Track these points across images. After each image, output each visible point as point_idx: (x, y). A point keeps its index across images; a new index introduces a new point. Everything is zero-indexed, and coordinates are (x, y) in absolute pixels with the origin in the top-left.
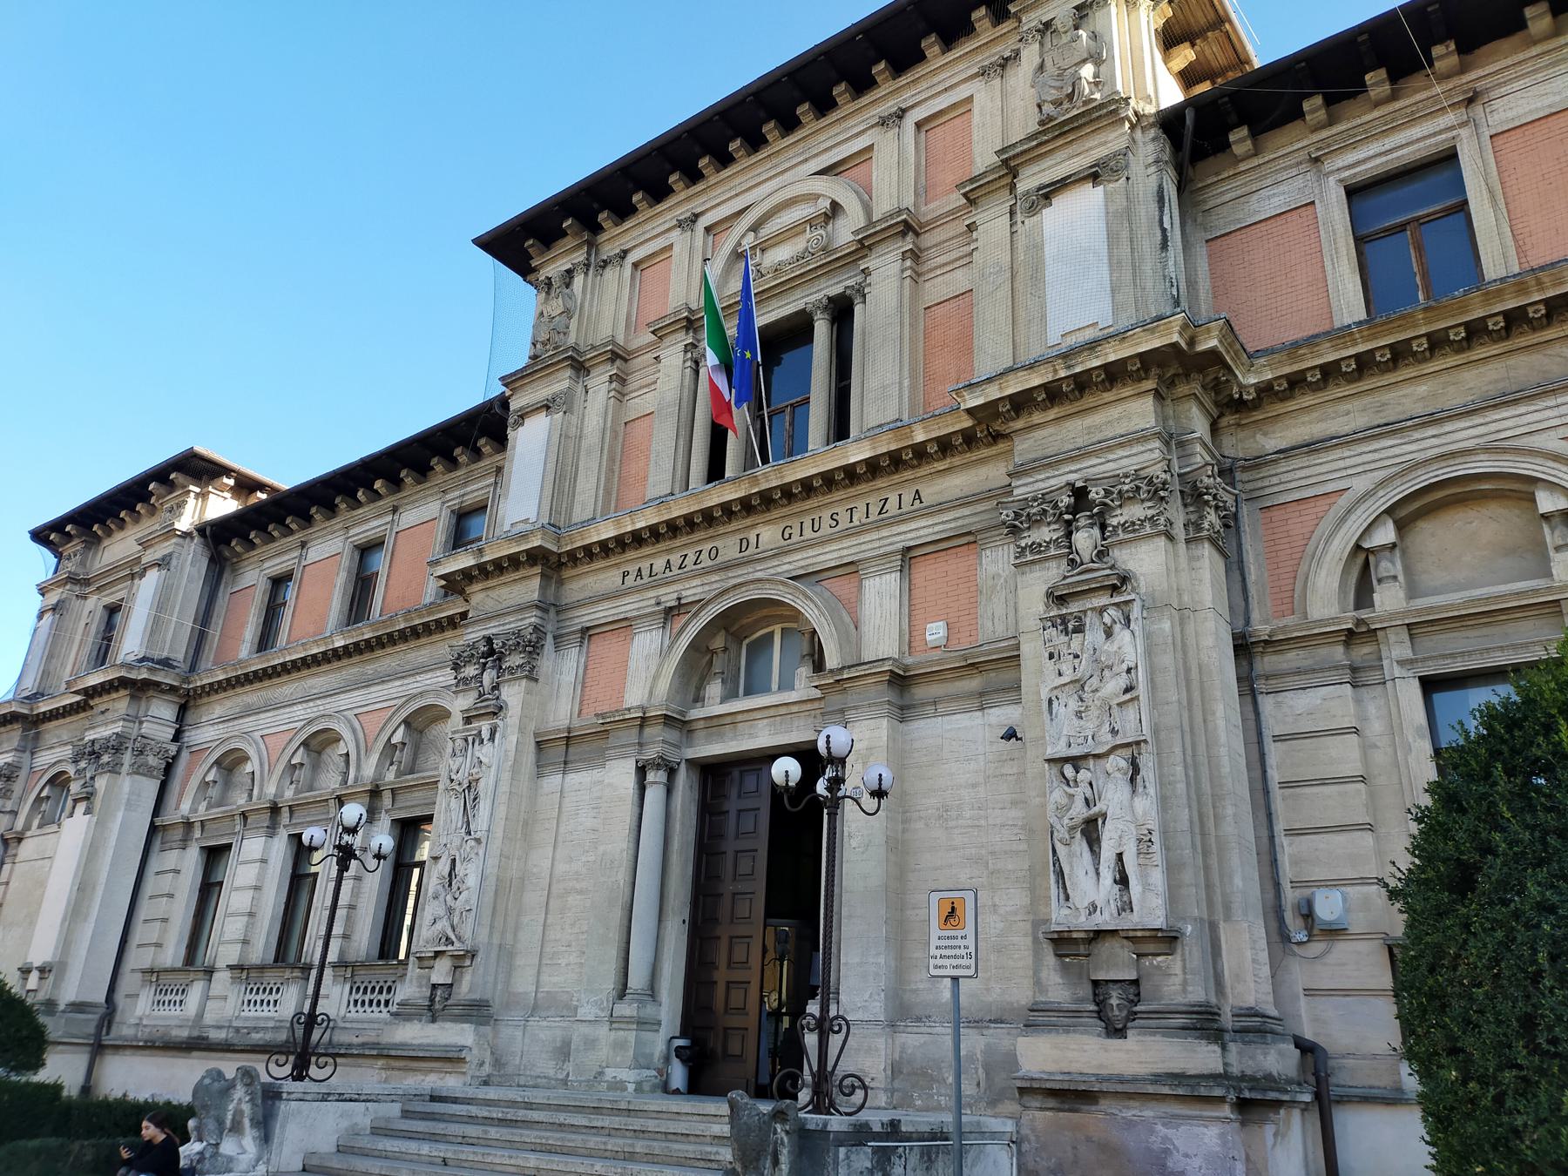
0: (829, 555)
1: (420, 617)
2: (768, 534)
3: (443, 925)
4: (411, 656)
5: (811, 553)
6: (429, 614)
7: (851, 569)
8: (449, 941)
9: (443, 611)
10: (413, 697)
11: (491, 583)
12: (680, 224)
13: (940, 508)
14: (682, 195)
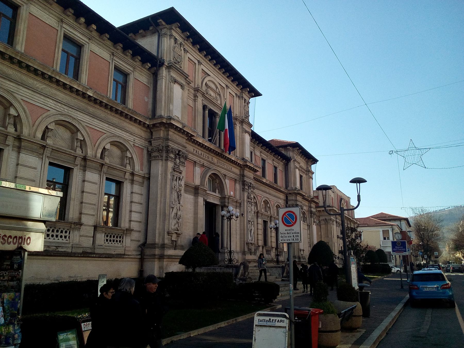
0: (223, 171)
1: (128, 111)
2: (215, 160)
3: (177, 226)
4: (54, 91)
5: (221, 169)
6: (131, 113)
7: (225, 175)
8: (178, 231)
9: (136, 116)
10: (115, 136)
11: (176, 132)
12: (198, 61)
13: (233, 173)
14: (201, 56)
